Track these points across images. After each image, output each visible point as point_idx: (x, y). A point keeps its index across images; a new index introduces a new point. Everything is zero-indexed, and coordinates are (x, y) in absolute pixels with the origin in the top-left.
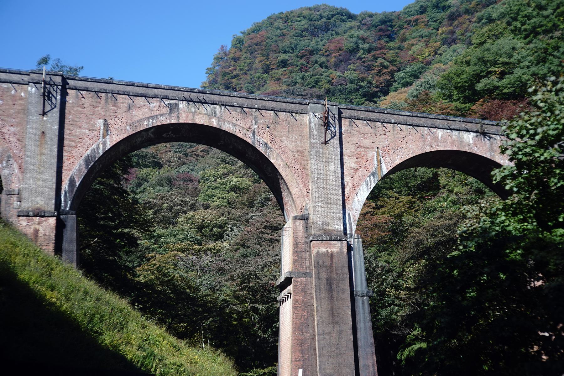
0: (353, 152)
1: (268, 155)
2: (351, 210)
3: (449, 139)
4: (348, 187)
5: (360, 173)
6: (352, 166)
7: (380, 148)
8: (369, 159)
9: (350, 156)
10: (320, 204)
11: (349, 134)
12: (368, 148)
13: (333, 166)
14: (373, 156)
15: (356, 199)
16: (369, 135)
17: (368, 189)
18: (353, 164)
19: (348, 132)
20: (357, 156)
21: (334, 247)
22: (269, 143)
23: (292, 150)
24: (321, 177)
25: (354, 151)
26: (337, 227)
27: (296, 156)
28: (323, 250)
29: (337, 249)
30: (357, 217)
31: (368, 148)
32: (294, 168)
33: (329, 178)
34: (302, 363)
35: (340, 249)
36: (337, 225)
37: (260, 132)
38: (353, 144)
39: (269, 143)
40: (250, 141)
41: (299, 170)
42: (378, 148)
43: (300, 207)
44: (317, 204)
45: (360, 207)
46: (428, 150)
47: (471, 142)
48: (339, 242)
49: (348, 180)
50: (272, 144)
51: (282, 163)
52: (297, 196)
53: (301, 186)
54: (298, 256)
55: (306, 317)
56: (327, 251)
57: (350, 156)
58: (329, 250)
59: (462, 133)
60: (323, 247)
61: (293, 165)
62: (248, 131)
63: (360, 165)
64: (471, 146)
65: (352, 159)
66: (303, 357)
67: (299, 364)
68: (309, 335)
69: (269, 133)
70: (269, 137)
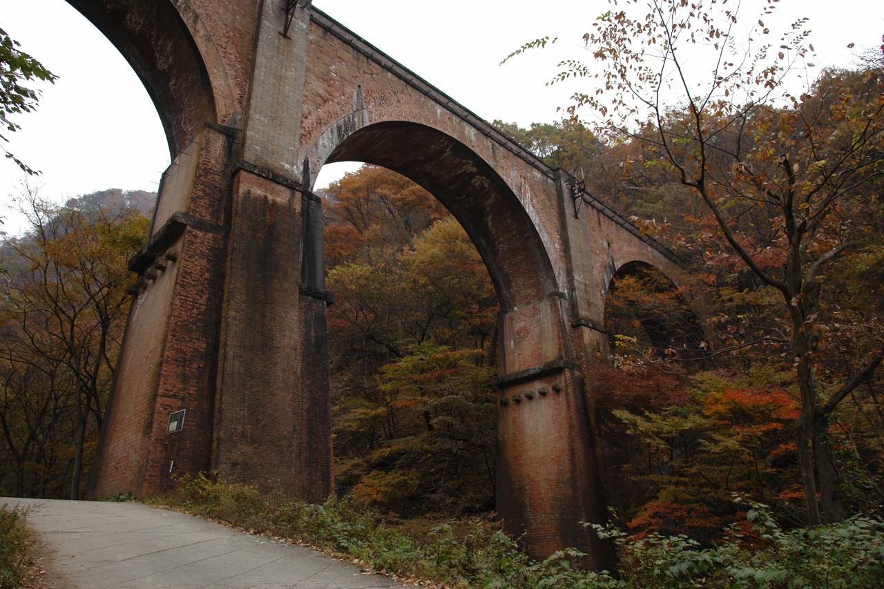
0: (324, 75)
3: (449, 121)
6: (320, 92)
13: (293, 74)
15: (321, 142)
21: (279, 195)
23: (226, 22)
25: (325, 73)
26: (287, 166)
28: (258, 192)
29: (283, 201)
32: (223, 50)
33: (284, 87)
35: (289, 201)
42: (359, 86)
43: (224, 113)
44: (257, 116)
49: (312, 110)
52: (220, 93)
53: (230, 80)
56: (266, 197)
58: (270, 197)
59: (464, 123)
60: (260, 186)
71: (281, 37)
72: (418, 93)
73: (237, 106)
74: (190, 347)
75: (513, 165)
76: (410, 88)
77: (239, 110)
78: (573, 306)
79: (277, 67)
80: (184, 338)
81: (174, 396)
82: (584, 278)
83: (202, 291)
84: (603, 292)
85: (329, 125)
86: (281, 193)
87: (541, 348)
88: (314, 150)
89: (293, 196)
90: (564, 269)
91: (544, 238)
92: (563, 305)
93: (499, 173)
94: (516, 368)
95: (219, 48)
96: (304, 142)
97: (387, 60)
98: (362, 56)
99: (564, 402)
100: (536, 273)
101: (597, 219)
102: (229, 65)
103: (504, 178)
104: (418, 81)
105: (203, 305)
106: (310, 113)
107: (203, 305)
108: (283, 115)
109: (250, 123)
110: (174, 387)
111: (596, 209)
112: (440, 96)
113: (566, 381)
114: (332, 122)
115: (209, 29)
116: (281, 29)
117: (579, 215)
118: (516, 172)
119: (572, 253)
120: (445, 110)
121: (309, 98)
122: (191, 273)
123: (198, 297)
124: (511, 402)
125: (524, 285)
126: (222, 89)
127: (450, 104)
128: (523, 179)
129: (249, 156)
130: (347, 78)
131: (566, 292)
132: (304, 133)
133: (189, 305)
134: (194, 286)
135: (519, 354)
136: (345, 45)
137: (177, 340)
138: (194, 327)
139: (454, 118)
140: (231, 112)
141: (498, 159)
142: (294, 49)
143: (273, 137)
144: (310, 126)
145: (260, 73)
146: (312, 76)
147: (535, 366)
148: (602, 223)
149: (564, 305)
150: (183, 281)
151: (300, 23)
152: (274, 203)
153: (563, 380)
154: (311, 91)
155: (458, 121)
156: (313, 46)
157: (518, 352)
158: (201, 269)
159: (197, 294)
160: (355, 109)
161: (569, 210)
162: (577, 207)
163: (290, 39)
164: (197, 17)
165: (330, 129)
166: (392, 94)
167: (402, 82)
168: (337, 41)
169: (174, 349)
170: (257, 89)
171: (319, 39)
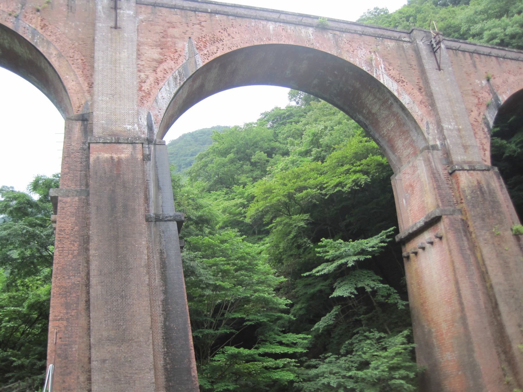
0: (156, 42)
1: (36, 43)
2: (152, 108)
3: (284, 33)
4: (148, 81)
5: (165, 66)
6: (154, 58)
7: (193, 38)
8: (179, 50)
9: (151, 46)
10: (104, 98)
11: (152, 22)
12: (177, 38)
13: (126, 54)
14: (184, 46)
15: (160, 96)
16: (178, 24)
17: (176, 84)
18: (156, 55)
19: (150, 19)
20: (162, 46)
21: (122, 152)
22: (39, 29)
24: (109, 65)
25: (158, 40)
26: (129, 127)
27: (76, 44)
28: (107, 155)
29: (127, 155)
30: (160, 117)
31: (177, 38)
32: (71, 59)
33: (120, 67)
34: (65, 323)
35: (132, 154)
36: (129, 125)
37: (27, 17)
38: (157, 33)
39: (39, 29)
40: (10, 25)
41: (80, 61)
43: (78, 105)
44: (100, 98)
45: (165, 106)
46: (256, 43)
47: (312, 37)
48: (130, 145)
50: (43, 30)
51: (55, 52)
52: (73, 91)
53: (80, 79)
54: (69, 168)
55: (76, 252)
56: (112, 157)
57: (151, 46)
58: (115, 156)
59: (298, 28)
61: (71, 55)
62: (10, 15)
63: (166, 57)
64: (312, 42)
65: (154, 50)
66: (67, 313)
67: (61, 325)
68: (79, 279)
69: (39, 18)
70: (39, 23)
71: (113, 30)
72: (248, 20)
73: (87, 94)
74: (69, 283)
75: (360, 45)
76: (239, 20)
77: (89, 98)
78: (447, 154)
79: (112, 55)
80: (64, 277)
81: (62, 319)
82: (456, 124)
83: (74, 241)
84: (486, 130)
85: (166, 80)
86: (124, 150)
87: (423, 201)
88: (155, 104)
89: (134, 149)
90: (433, 122)
91: (405, 100)
92: (436, 156)
93: (344, 58)
94: (411, 224)
95: (69, 59)
96: (145, 102)
97: (213, 6)
98: (190, 12)
99: (447, 248)
100: (409, 133)
101: (470, 62)
102: (78, 68)
103: (351, 60)
104: (247, 10)
105: (76, 250)
106: (147, 78)
107: (76, 250)
108: (121, 89)
109: (95, 105)
110: (61, 313)
111: (468, 52)
112: (271, 14)
113: (445, 228)
114: (168, 77)
115: (59, 48)
116: (112, 24)
117: (442, 66)
118: (364, 50)
119: (438, 105)
120: (278, 24)
121: (146, 65)
122: (64, 230)
123: (72, 246)
124: (412, 256)
125: (403, 146)
126: (74, 88)
127: (283, 17)
128: (373, 54)
129: (97, 131)
130: (177, 35)
131: (438, 143)
132: (144, 94)
133: (65, 253)
134: (68, 238)
135: (410, 210)
136: (173, 10)
137: (59, 280)
138: (71, 268)
139: (288, 27)
140: (83, 102)
141: (342, 45)
142: (125, 34)
143: (115, 109)
144: (148, 88)
145: (99, 65)
146: (147, 48)
147: (420, 222)
148: (477, 63)
149: (438, 154)
150: (60, 237)
151: (128, 12)
152: (120, 160)
153: (442, 227)
154: (146, 60)
155: (293, 28)
156: (144, 23)
157: (409, 208)
158: (72, 225)
159: (70, 244)
160: (187, 58)
161: (429, 64)
162: (438, 57)
163: (120, 28)
164: (49, 43)
165: (167, 83)
166: (222, 31)
167: (231, 17)
168: (164, 11)
169: (57, 287)
170: (98, 78)
171: (149, 15)
